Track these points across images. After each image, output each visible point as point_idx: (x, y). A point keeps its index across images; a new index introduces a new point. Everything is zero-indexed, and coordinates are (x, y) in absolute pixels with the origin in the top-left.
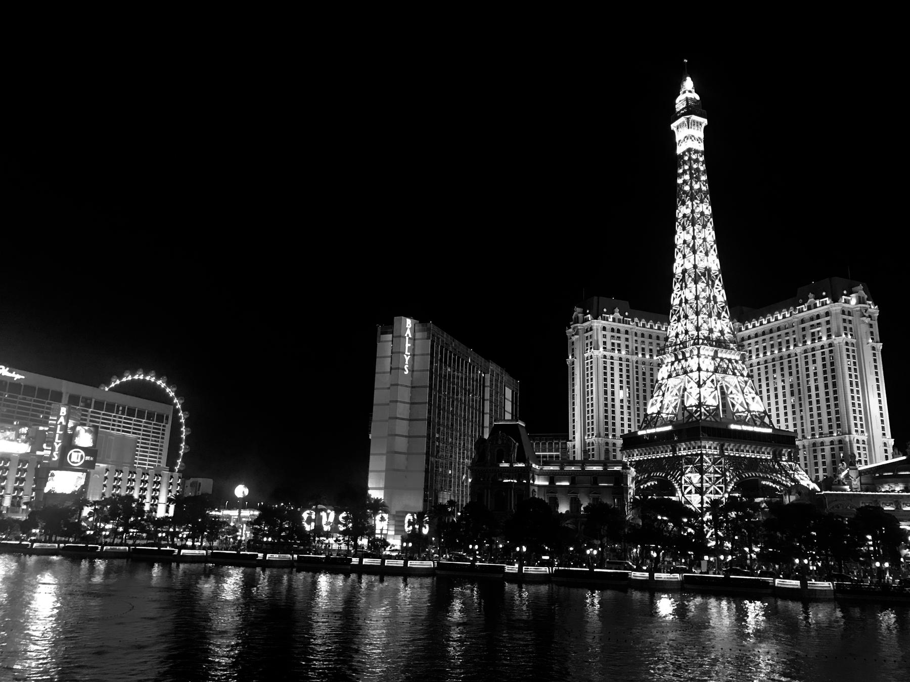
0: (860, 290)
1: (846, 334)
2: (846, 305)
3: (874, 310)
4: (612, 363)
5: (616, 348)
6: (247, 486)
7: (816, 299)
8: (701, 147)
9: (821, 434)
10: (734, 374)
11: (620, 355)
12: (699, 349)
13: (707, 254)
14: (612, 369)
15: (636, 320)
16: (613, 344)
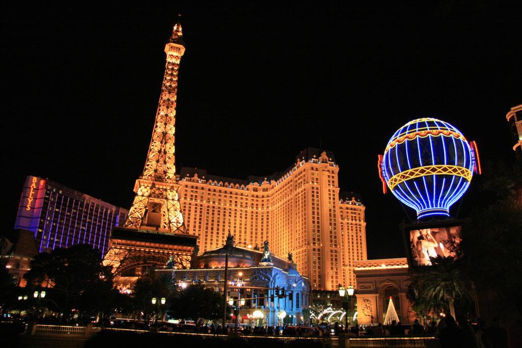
0: (324, 155)
1: (313, 182)
2: (314, 164)
3: (336, 169)
4: (190, 207)
5: (194, 198)
6: (151, 300)
7: (301, 161)
8: (178, 62)
9: (299, 246)
10: (166, 198)
11: (196, 203)
12: (140, 181)
13: (166, 124)
14: (190, 211)
15: (210, 181)
16: (192, 196)
